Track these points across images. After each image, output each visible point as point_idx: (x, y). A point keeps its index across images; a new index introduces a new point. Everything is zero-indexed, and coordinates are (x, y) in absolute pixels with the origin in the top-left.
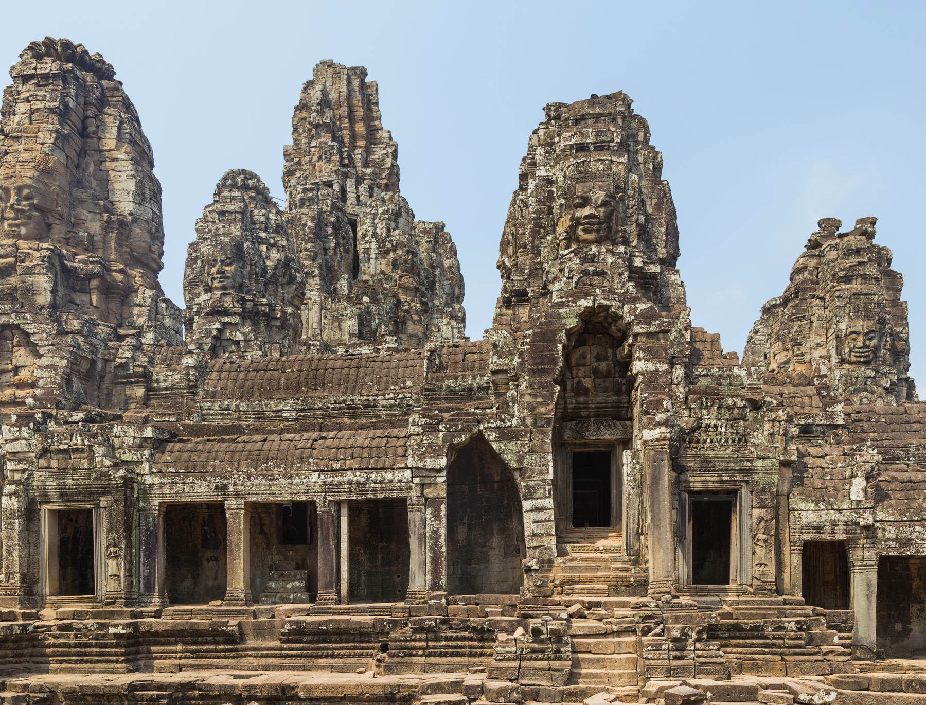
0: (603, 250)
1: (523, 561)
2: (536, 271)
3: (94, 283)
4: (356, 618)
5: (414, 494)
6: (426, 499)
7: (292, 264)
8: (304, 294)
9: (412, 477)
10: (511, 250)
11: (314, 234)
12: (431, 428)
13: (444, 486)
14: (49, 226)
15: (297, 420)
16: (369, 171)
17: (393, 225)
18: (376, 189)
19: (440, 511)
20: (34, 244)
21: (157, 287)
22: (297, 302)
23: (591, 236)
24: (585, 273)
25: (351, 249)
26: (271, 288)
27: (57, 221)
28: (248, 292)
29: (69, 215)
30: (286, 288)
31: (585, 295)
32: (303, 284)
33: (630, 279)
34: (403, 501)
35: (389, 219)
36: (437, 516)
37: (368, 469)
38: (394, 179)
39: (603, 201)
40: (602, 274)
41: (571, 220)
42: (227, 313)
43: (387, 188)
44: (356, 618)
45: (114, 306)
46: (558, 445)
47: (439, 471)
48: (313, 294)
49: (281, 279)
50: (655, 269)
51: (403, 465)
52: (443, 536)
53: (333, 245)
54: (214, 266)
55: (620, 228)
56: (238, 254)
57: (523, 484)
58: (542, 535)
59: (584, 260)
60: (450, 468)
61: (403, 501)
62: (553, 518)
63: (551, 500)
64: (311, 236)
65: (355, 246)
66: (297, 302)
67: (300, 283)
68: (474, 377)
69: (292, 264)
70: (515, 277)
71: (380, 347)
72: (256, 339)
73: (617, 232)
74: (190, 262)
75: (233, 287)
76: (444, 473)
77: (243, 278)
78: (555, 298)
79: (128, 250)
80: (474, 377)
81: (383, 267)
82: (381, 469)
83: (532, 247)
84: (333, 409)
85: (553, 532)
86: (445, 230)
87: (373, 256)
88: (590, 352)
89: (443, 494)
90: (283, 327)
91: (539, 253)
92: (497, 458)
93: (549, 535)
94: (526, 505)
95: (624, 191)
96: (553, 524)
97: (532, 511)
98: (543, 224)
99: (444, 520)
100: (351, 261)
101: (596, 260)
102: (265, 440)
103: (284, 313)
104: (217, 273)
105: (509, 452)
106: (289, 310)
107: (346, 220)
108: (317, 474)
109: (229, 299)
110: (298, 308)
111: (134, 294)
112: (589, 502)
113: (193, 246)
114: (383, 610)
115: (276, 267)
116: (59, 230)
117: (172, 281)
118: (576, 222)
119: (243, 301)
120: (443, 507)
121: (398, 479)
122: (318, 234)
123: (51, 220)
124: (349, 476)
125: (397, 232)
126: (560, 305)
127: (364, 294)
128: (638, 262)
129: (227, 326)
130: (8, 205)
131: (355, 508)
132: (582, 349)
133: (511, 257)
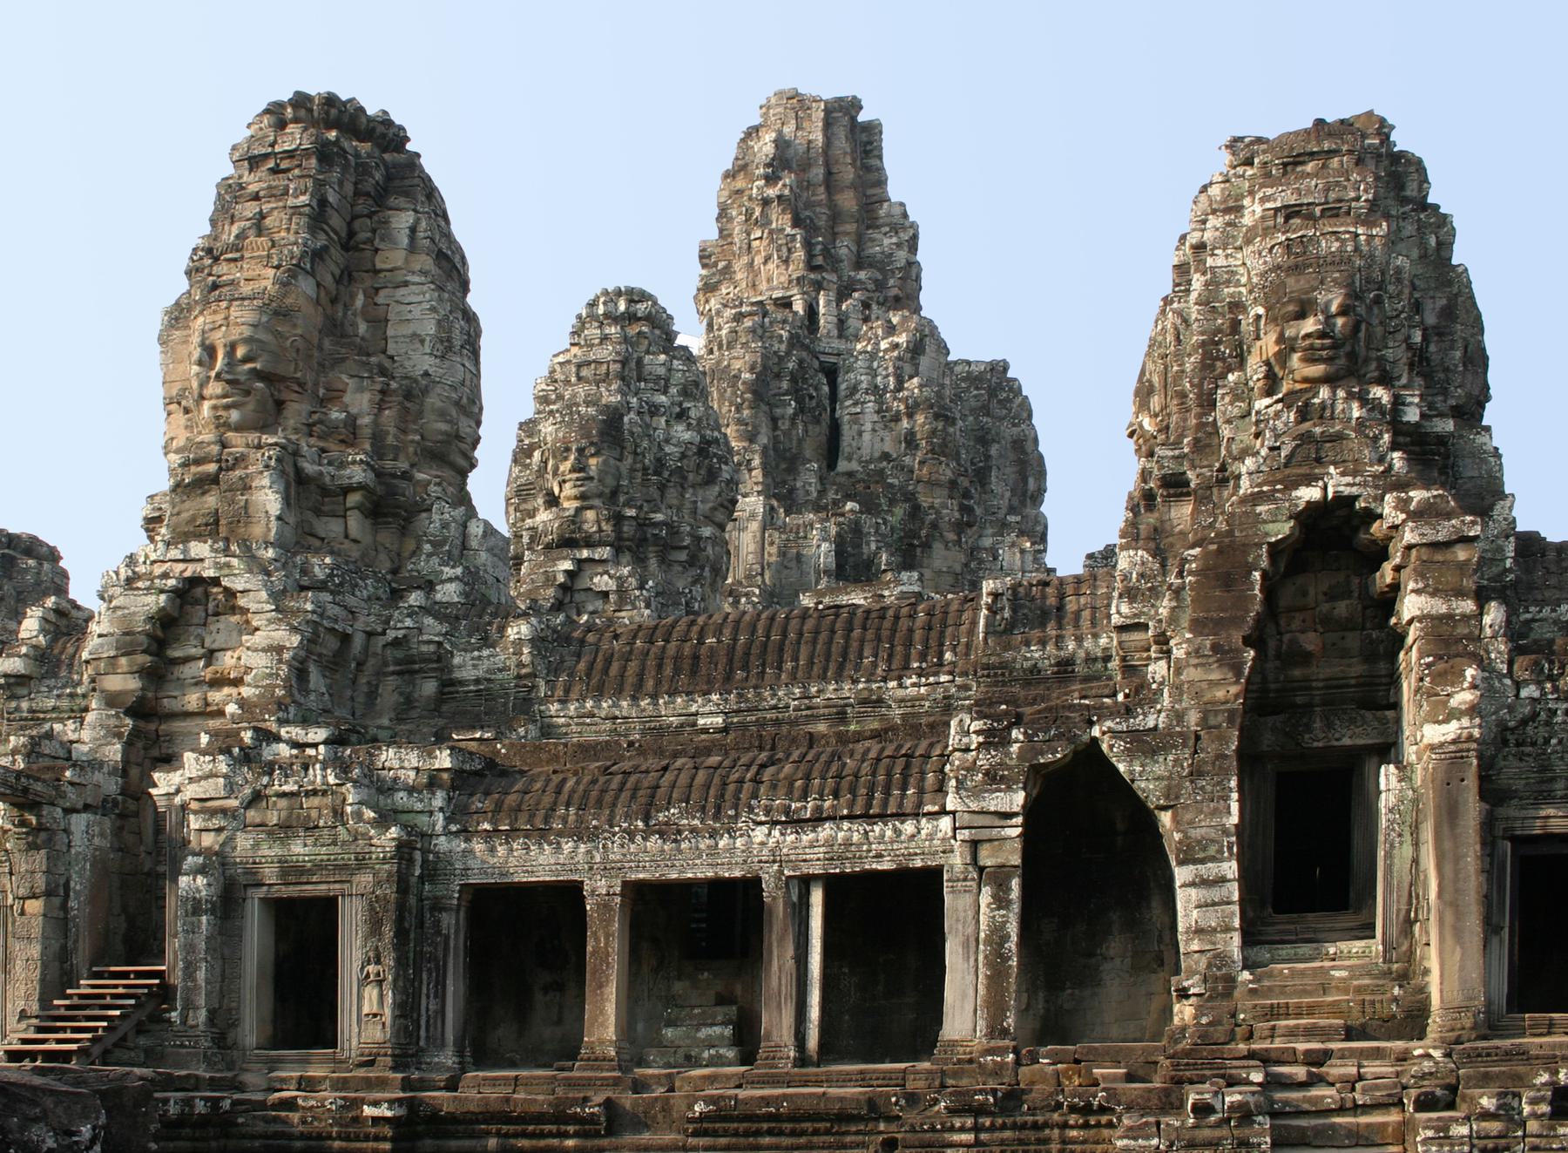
0: (1341, 394)
1: (1174, 979)
2: (1206, 440)
3: (354, 499)
4: (834, 1091)
5: (958, 860)
6: (981, 869)
7: (713, 449)
8: (734, 502)
9: (955, 829)
10: (1156, 402)
11: (754, 392)
12: (995, 739)
13: (1018, 845)
14: (280, 405)
15: (725, 730)
16: (862, 275)
17: (908, 368)
18: (874, 307)
19: (1010, 889)
20: (252, 437)
21: (464, 499)
22: (720, 516)
23: (1317, 370)
24: (1305, 438)
25: (826, 417)
26: (672, 494)
27: (294, 396)
28: (628, 504)
29: (316, 384)
30: (700, 492)
31: (1309, 480)
32: (733, 484)
33: (1394, 446)
34: (933, 877)
35: (899, 358)
36: (1001, 901)
37: (867, 817)
38: (911, 284)
39: (1340, 306)
40: (1339, 437)
41: (1278, 342)
42: (589, 544)
43: (896, 303)
44: (834, 1091)
45: (387, 537)
46: (1249, 761)
47: (1009, 815)
48: (752, 503)
49: (691, 476)
50: (1449, 425)
51: (936, 808)
52: (1014, 938)
53: (790, 411)
54: (566, 459)
55: (1374, 354)
56: (610, 431)
57: (1177, 836)
58: (1215, 930)
59: (1303, 415)
60: (1029, 810)
61: (933, 877)
62: (1236, 897)
63: (1234, 864)
64: (748, 396)
65: (833, 410)
66: (720, 516)
67: (728, 482)
68: (1079, 640)
69: (713, 449)
70: (1159, 451)
71: (886, 593)
72: (641, 587)
73: (1367, 361)
74: (522, 455)
75: (600, 495)
76: (1019, 820)
77: (619, 477)
78: (1245, 485)
79: (417, 438)
80: (1079, 640)
81: (888, 446)
82: (892, 815)
83: (1199, 396)
84: (797, 709)
85: (1237, 923)
86: (1010, 374)
87: (868, 426)
88: (1316, 585)
89: (1016, 860)
90: (692, 561)
91: (1213, 405)
92: (1122, 789)
93: (1228, 929)
94: (1181, 874)
95: (1381, 286)
96: (1236, 908)
97: (1192, 884)
98: (1220, 350)
99: (1016, 907)
100: (824, 439)
101: (1328, 413)
102: (665, 769)
103: (698, 539)
104: (573, 470)
105: (1148, 778)
106: (707, 531)
107: (816, 364)
108: (765, 829)
109: (590, 515)
110: (722, 528)
111: (424, 515)
112: (1309, 865)
113: (528, 427)
114: (887, 1078)
115: (683, 456)
116: (297, 410)
117: (489, 488)
118: (1287, 347)
119: (618, 519)
120: (1015, 884)
121: (928, 837)
122: (761, 392)
123: (286, 395)
124: (826, 831)
125: (915, 380)
126: (1256, 498)
127: (849, 497)
128: (1412, 415)
129: (586, 566)
130: (213, 374)
131: (837, 887)
132: (1300, 580)
133: (1156, 415)
